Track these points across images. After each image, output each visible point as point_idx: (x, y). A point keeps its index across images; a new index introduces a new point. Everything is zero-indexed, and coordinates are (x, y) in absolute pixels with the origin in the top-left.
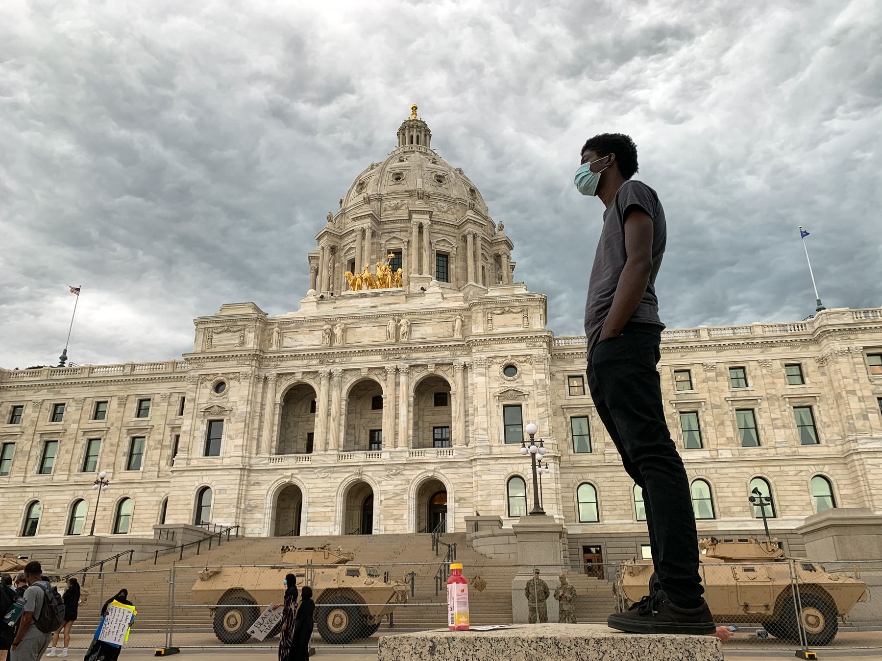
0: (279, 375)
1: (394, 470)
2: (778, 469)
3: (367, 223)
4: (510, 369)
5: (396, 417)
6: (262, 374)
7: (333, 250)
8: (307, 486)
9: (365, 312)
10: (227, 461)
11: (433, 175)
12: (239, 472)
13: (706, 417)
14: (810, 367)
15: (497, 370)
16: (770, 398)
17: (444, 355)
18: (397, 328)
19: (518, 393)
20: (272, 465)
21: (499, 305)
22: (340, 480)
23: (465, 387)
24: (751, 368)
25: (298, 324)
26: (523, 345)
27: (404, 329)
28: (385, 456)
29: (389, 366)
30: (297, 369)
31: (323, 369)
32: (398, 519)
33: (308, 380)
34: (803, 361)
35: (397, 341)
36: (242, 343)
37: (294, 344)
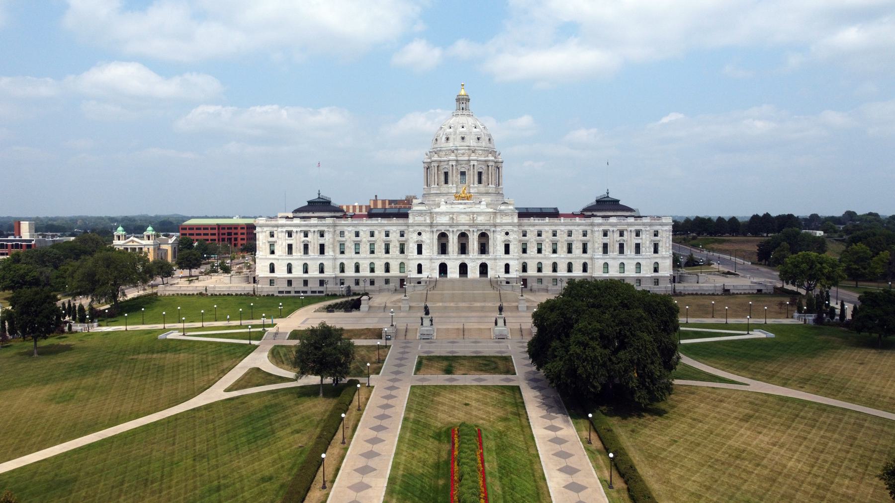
1: (473, 260)
3: (454, 163)
4: (507, 234)
5: (473, 245)
7: (438, 167)
9: (463, 211)
10: (424, 257)
11: (476, 137)
13: (559, 245)
14: (589, 232)
15: (503, 233)
16: (577, 240)
17: (487, 227)
18: (473, 218)
19: (509, 241)
20: (438, 257)
23: (494, 237)
24: (574, 232)
25: (441, 213)
26: (511, 227)
28: (471, 256)
29: (471, 229)
30: (443, 229)
31: (451, 229)
32: (475, 273)
36: (425, 220)
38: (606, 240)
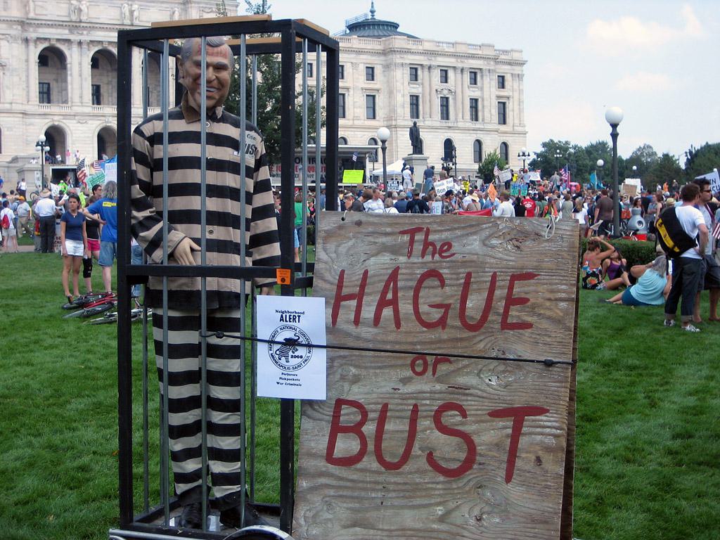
0: (38, 39)
2: (352, 133)
6: (26, 35)
8: (71, 128)
12: (21, 115)
14: (378, 71)
18: (132, 12)
21: (208, 6)
22: (94, 126)
27: (136, 14)
33: (59, 45)
34: (375, 66)
35: (132, 20)
37: (44, 12)
38: (416, 90)
